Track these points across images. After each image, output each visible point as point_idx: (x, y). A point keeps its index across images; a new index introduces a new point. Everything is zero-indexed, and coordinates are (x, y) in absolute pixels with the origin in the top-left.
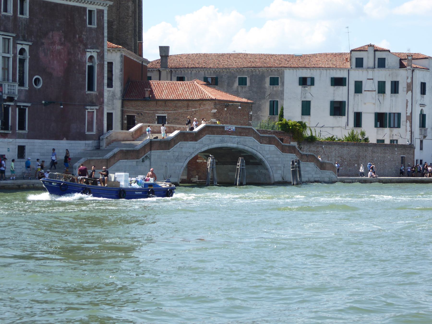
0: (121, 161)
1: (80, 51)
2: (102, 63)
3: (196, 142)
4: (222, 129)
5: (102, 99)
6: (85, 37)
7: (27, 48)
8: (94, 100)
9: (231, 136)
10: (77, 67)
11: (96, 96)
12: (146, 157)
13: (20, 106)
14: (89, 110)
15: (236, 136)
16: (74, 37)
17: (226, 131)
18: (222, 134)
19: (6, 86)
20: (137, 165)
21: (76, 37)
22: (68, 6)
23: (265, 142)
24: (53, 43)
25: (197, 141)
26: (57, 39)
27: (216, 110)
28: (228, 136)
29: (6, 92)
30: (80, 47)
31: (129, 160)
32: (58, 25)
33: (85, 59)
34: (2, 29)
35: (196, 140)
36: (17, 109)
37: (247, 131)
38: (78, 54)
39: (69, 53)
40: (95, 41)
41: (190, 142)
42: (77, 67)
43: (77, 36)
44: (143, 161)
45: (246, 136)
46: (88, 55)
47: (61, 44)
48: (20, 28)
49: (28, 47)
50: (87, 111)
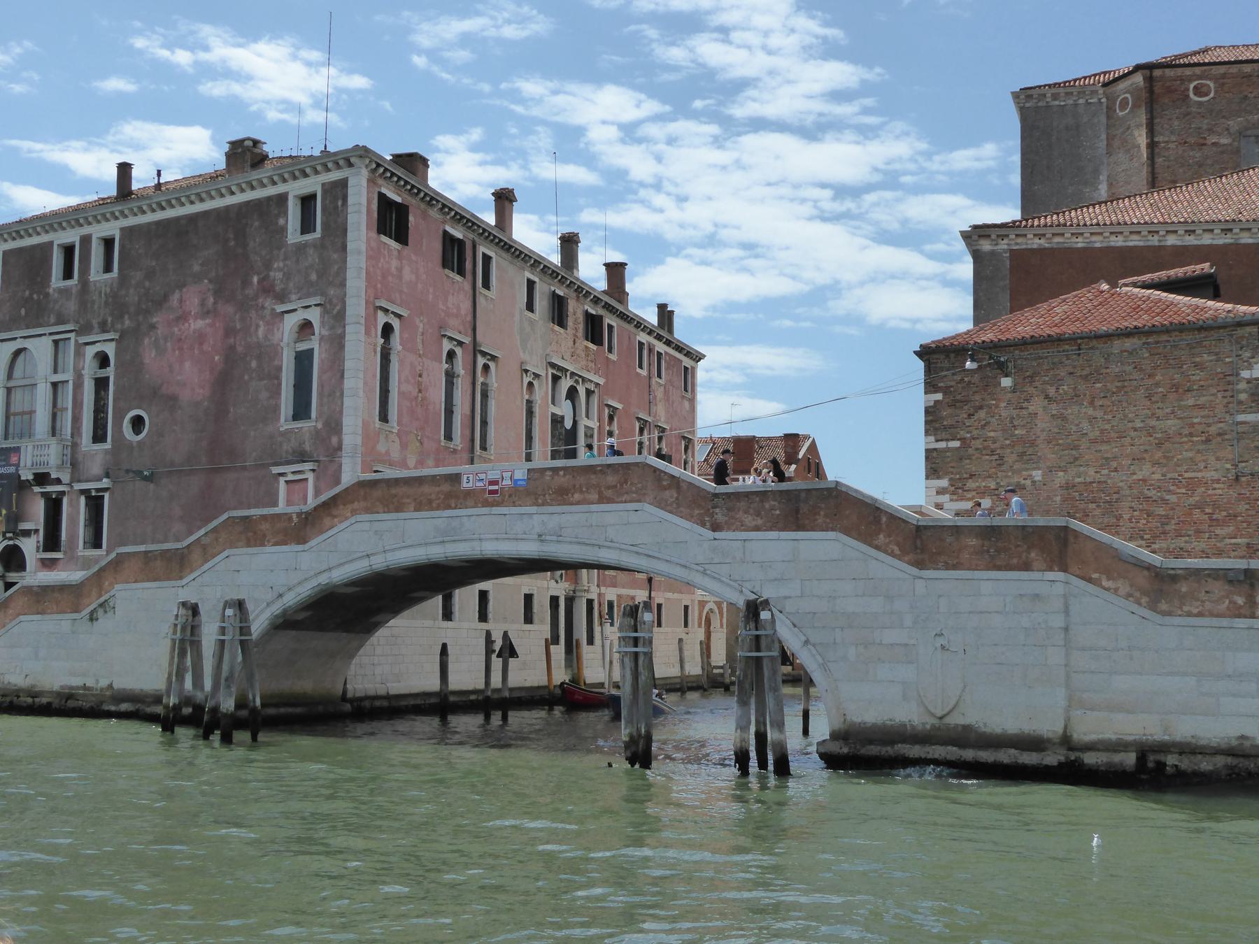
0: (22, 618)
1: (262, 318)
2: (339, 331)
3: (300, 547)
4: (446, 487)
5: (334, 440)
6: (279, 275)
7: (110, 349)
8: (307, 447)
9: (496, 510)
10: (254, 364)
11: (316, 434)
12: (101, 605)
13: (88, 491)
14: (291, 477)
15: (534, 509)
16: (246, 283)
17: (469, 493)
18: (449, 507)
19: (30, 448)
20: (73, 632)
21: (251, 283)
22: (227, 209)
23: (749, 520)
24: (183, 318)
25: (305, 542)
26: (193, 303)
27: (939, 396)
28: (485, 510)
29: (29, 464)
30: (263, 307)
31: (47, 617)
32: (196, 268)
33: (277, 336)
34: (52, 320)
35: (302, 540)
36: (83, 500)
37: (611, 479)
38: (258, 326)
39: (229, 332)
40: (314, 277)
41: (268, 549)
42: (254, 364)
43: (255, 279)
44: (92, 618)
45: (602, 499)
46: (291, 322)
47: (205, 313)
48: (96, 306)
49: (113, 344)
50: (282, 480)
